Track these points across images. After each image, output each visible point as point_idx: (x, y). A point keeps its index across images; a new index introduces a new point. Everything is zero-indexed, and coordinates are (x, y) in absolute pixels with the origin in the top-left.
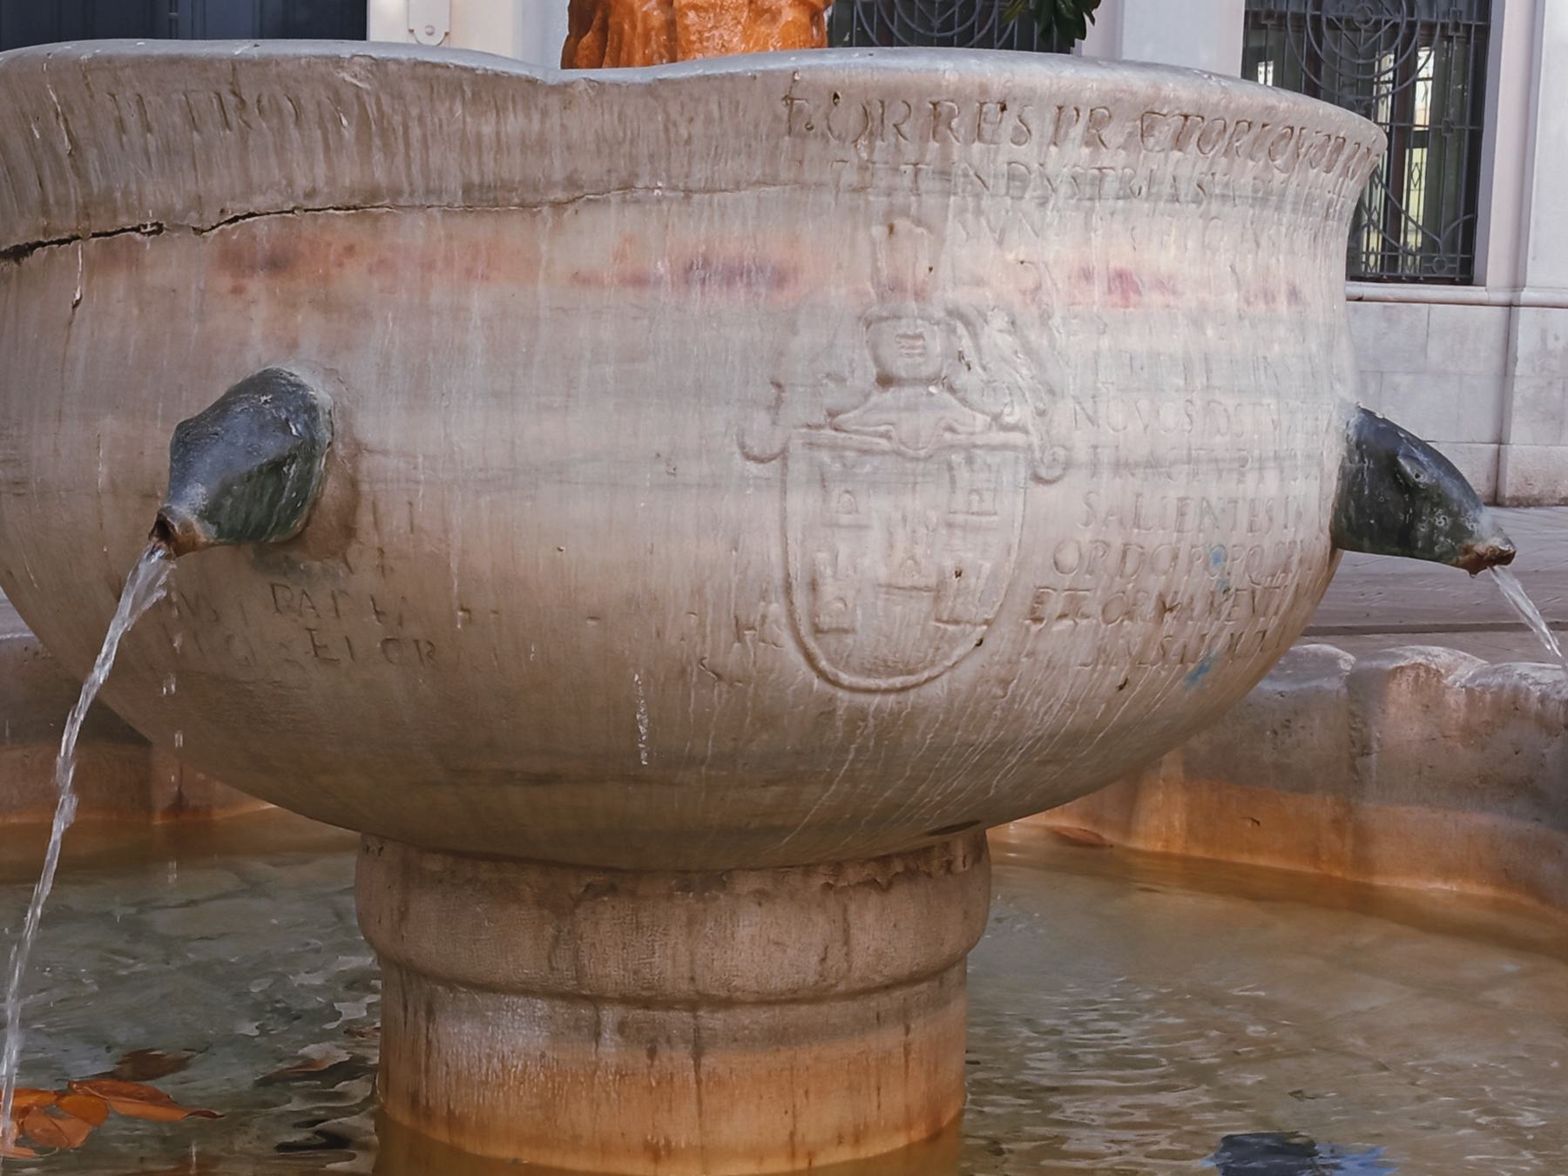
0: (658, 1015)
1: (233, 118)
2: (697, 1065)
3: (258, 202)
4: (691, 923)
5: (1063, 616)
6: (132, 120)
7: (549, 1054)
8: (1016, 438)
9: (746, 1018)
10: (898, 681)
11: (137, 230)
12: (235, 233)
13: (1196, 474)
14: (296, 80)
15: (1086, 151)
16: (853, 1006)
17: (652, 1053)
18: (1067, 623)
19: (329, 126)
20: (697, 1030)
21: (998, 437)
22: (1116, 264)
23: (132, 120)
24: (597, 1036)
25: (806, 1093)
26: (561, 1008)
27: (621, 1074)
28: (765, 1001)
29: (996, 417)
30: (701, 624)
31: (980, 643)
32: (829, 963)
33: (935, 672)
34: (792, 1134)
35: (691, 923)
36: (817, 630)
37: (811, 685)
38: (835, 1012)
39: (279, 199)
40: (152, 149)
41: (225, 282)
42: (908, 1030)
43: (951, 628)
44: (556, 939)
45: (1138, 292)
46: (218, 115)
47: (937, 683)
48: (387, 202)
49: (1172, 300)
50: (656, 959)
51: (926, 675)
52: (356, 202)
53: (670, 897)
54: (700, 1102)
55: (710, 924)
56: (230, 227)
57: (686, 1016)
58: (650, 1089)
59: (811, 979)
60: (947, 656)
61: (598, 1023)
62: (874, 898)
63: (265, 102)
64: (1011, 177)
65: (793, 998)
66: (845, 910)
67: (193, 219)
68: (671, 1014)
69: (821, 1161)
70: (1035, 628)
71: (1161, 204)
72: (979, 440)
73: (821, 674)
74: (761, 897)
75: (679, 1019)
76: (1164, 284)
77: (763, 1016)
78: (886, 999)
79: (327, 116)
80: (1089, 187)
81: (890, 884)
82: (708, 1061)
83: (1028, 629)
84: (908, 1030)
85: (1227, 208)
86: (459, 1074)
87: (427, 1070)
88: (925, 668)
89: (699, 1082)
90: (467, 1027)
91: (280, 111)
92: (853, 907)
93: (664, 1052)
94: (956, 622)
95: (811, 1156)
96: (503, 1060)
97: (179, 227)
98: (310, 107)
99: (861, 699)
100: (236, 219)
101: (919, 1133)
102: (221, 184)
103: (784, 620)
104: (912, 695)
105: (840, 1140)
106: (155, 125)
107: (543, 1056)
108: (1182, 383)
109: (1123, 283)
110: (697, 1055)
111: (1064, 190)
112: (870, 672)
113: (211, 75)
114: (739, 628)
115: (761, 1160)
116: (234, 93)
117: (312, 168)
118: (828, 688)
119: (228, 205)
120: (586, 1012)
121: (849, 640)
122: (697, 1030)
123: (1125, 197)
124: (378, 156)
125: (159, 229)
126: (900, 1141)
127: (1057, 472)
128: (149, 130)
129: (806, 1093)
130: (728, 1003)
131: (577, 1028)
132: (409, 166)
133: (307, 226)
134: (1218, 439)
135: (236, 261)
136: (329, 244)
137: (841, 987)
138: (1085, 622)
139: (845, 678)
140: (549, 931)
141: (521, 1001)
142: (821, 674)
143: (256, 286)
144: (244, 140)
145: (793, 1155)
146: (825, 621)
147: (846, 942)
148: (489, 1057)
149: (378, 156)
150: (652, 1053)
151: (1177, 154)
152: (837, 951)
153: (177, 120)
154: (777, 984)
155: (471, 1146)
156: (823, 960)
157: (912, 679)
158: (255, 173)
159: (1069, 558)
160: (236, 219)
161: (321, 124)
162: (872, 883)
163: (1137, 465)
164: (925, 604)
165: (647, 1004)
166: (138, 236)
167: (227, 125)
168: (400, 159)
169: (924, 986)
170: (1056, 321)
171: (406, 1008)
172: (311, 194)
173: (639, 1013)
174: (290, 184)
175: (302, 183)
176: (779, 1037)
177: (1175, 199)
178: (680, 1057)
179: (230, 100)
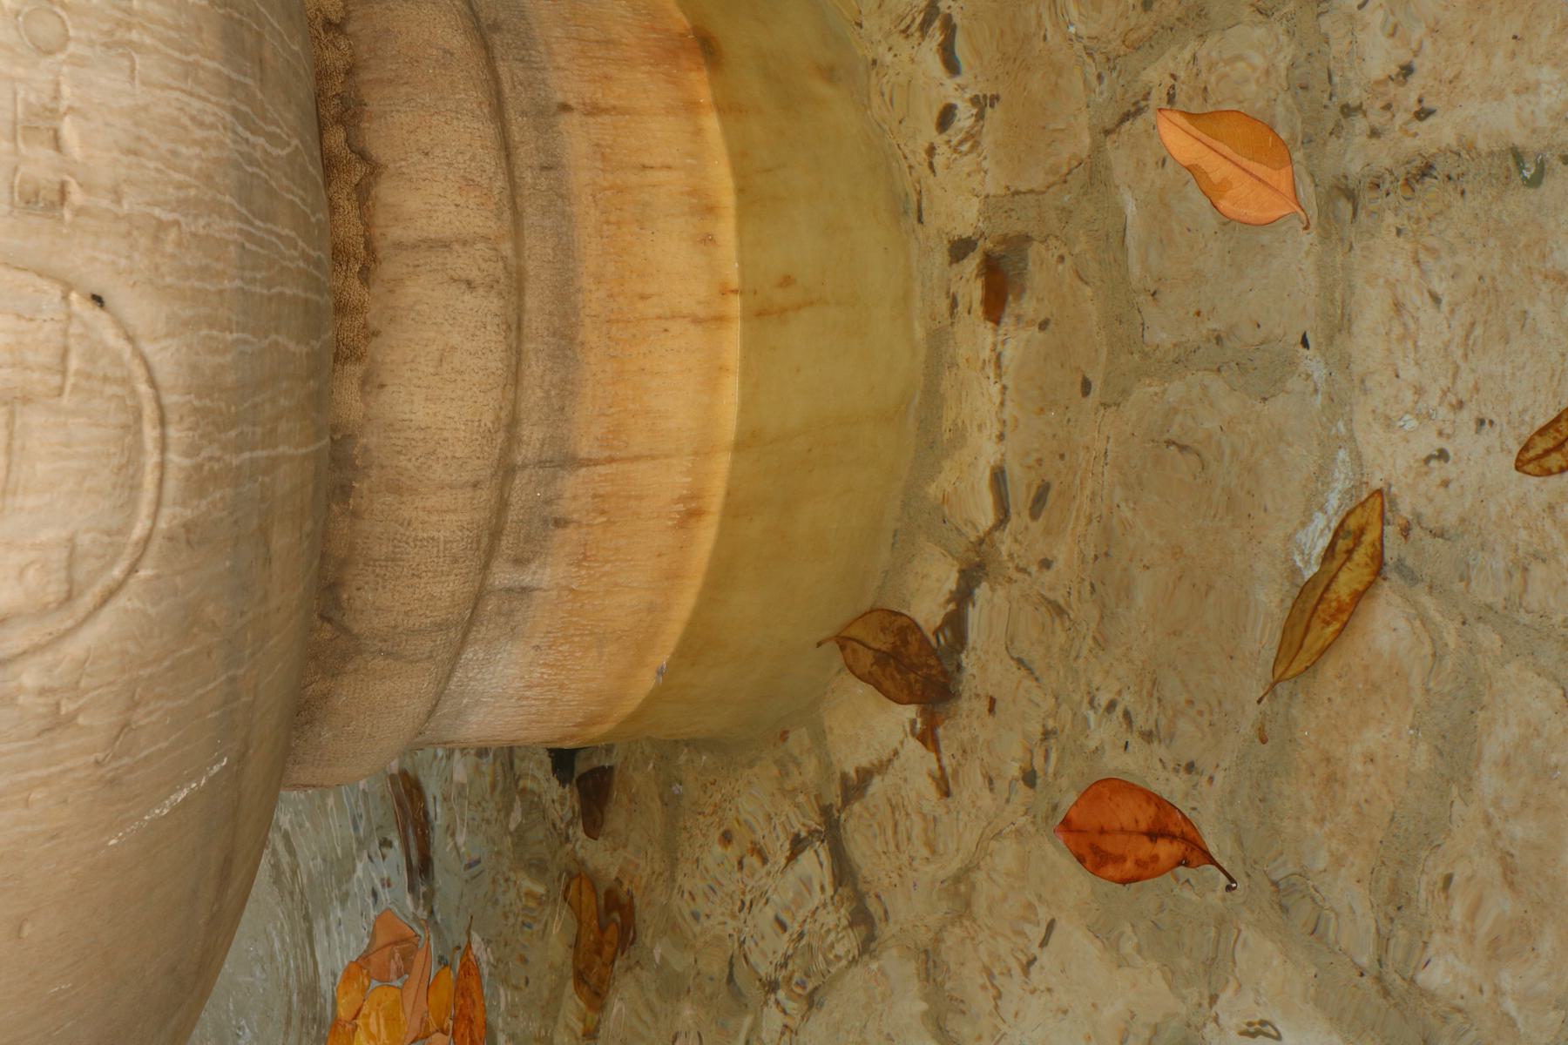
0: (513, 515)
2: (590, 462)
4: (397, 489)
5: (57, 142)
7: (536, 642)
9: (533, 396)
10: (150, 433)
16: (531, 216)
17: (560, 523)
18: (69, 130)
20: (541, 463)
24: (525, 590)
25: (643, 297)
27: (583, 559)
28: (515, 375)
30: (45, 782)
31: (98, 300)
32: (474, 274)
33: (139, 372)
34: (697, 321)
35: (397, 489)
36: (69, 597)
37: (148, 580)
38: (538, 250)
42: (565, 108)
43: (74, 363)
44: (388, 655)
47: (155, 360)
50: (441, 535)
51: (143, 388)
53: (356, 515)
54: (637, 458)
55: (403, 461)
57: (520, 480)
58: (610, 522)
59: (495, 304)
60: (117, 359)
61: (509, 590)
62: (386, 191)
65: (515, 327)
66: (399, 246)
68: (513, 500)
69: (733, 276)
70: (76, 196)
73: (133, 569)
74: (370, 383)
75: (523, 490)
77: (535, 368)
78: (522, 151)
81: (363, 156)
82: (585, 449)
83: (80, 211)
84: (565, 108)
86: (530, 722)
88: (134, 392)
89: (611, 460)
92: (396, 233)
93: (562, 508)
94: (64, 354)
95: (725, 291)
99: (171, 486)
101: (700, 85)
103: (49, 657)
104: (170, 399)
105: (708, 240)
110: (572, 462)
112: (135, 488)
114: (58, 722)
115: (722, 369)
118: (154, 547)
120: (491, 605)
121: (85, 540)
122: (541, 463)
129: (643, 297)
130: (512, 424)
131: (511, 613)
137: (507, 248)
138: (66, 90)
139: (139, 531)
140: (380, 663)
141: (459, 674)
142: (133, 569)
145: (720, 319)
146: (55, 590)
147: (446, 245)
150: (560, 523)
152: (463, 263)
154: (495, 362)
156: (469, 284)
157: (149, 411)
162: (363, 193)
164: (34, 418)
165: (496, 534)
169: (503, 69)
173: (506, 542)
176: (566, 341)
178: (572, 485)
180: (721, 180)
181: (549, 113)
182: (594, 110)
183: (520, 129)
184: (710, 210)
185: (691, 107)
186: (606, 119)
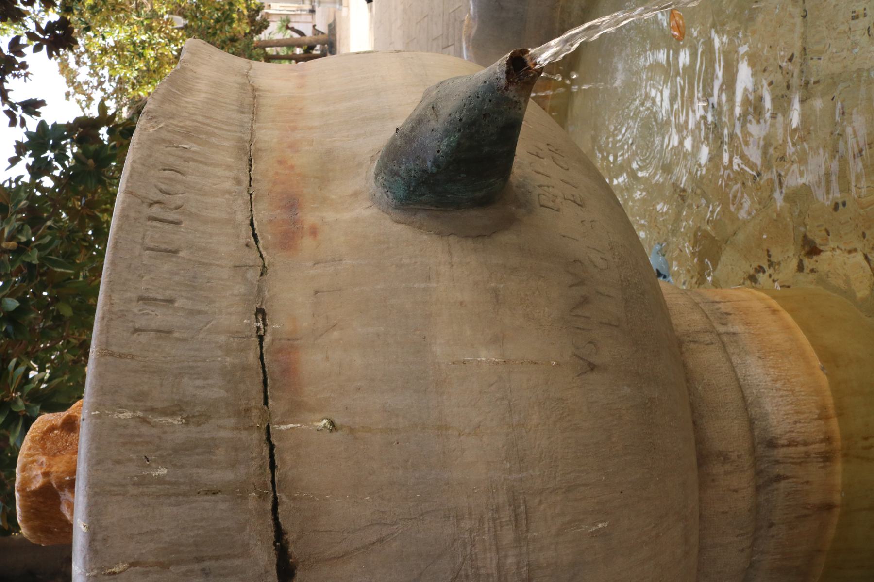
1: (173, 216)
3: (242, 217)
6: (159, 317)
7: (757, 354)
11: (261, 338)
12: (267, 236)
14: (150, 156)
19: (187, 155)
23: (159, 317)
26: (731, 349)
39: (240, 201)
40: (189, 305)
41: (307, 243)
46: (168, 227)
48: (247, 145)
52: (246, 158)
56: (261, 242)
63: (163, 187)
67: (253, 275)
79: (180, 153)
87: (805, 444)
90: (769, 408)
91: (171, 180)
96: (775, 381)
97: (260, 290)
98: (171, 160)
100: (255, 235)
102: (227, 245)
106: (168, 294)
107: (760, 358)
113: (133, 215)
116: (151, 205)
117: (219, 177)
119: (243, 241)
124: (213, 140)
125: (261, 313)
128: (171, 301)
132: (221, 129)
133: (261, 186)
135: (288, 239)
136: (277, 173)
143: (310, 218)
144: (191, 214)
148: (778, 390)
149: (213, 140)
153: (166, 267)
155: (830, 402)
158: (215, 214)
160: (255, 235)
161: (187, 160)
166: (267, 339)
167: (177, 223)
168: (216, 131)
171: (779, 478)
172: (238, 182)
174: (229, 192)
175: (228, 185)
179: (155, 210)
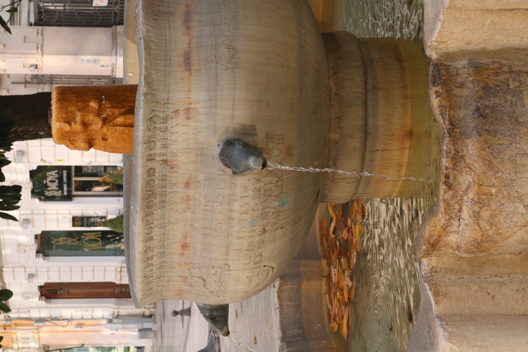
5: (261, 255)
8: (219, 272)
13: (231, 235)
15: (154, 258)
18: (263, 254)
21: (218, 274)
22: (180, 248)
29: (214, 274)
31: (265, 266)
42: (378, 150)
45: (186, 243)
49: (189, 235)
64: (160, 268)
66: (338, 179)
71: (166, 237)
72: (218, 277)
76: (185, 237)
80: (162, 254)
84: (378, 150)
85: (166, 217)
92: (338, 177)
108: (209, 237)
109: (184, 246)
111: (163, 259)
123: (164, 246)
126: (407, 152)
127: (227, 266)
134: (223, 227)
147: (347, 179)
151: (154, 237)
152: (348, 180)
159: (248, 261)
163: (227, 251)
169: (368, 144)
170: (193, 261)
177: (164, 234)
180: (405, 160)
181: (373, 152)
182: (384, 150)
183: (368, 155)
184: (401, 166)
185: (403, 149)
186: (385, 152)
